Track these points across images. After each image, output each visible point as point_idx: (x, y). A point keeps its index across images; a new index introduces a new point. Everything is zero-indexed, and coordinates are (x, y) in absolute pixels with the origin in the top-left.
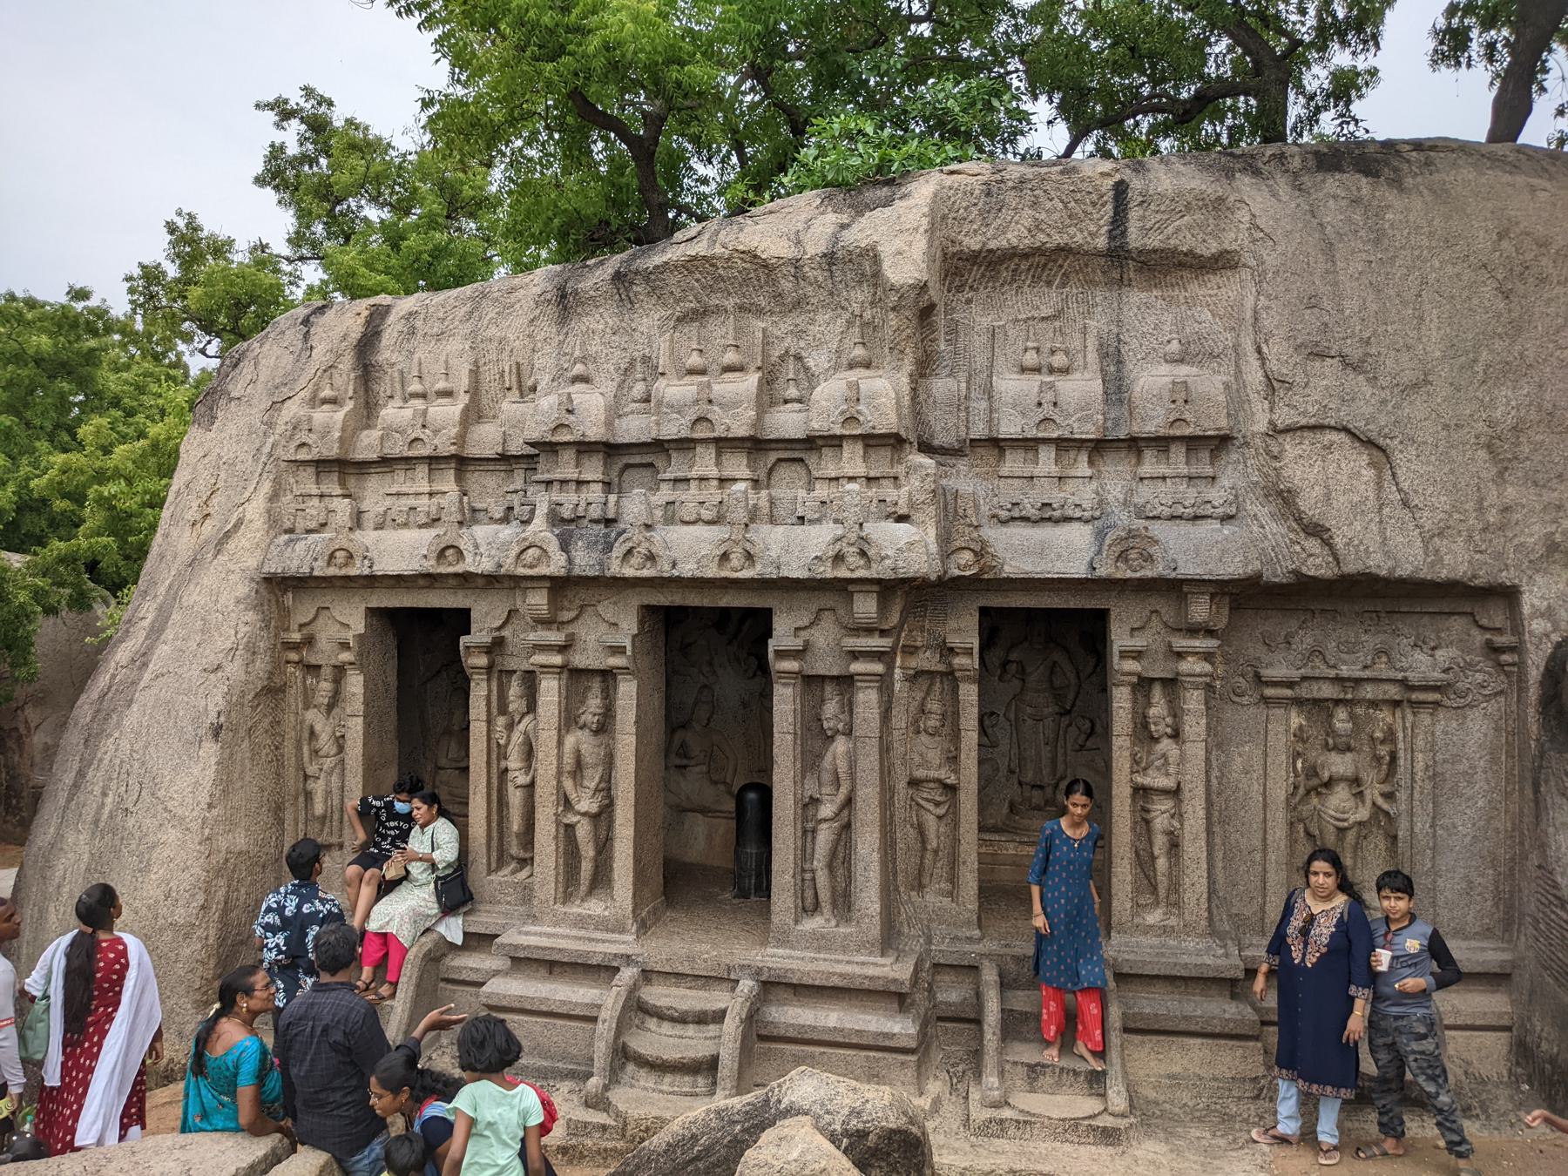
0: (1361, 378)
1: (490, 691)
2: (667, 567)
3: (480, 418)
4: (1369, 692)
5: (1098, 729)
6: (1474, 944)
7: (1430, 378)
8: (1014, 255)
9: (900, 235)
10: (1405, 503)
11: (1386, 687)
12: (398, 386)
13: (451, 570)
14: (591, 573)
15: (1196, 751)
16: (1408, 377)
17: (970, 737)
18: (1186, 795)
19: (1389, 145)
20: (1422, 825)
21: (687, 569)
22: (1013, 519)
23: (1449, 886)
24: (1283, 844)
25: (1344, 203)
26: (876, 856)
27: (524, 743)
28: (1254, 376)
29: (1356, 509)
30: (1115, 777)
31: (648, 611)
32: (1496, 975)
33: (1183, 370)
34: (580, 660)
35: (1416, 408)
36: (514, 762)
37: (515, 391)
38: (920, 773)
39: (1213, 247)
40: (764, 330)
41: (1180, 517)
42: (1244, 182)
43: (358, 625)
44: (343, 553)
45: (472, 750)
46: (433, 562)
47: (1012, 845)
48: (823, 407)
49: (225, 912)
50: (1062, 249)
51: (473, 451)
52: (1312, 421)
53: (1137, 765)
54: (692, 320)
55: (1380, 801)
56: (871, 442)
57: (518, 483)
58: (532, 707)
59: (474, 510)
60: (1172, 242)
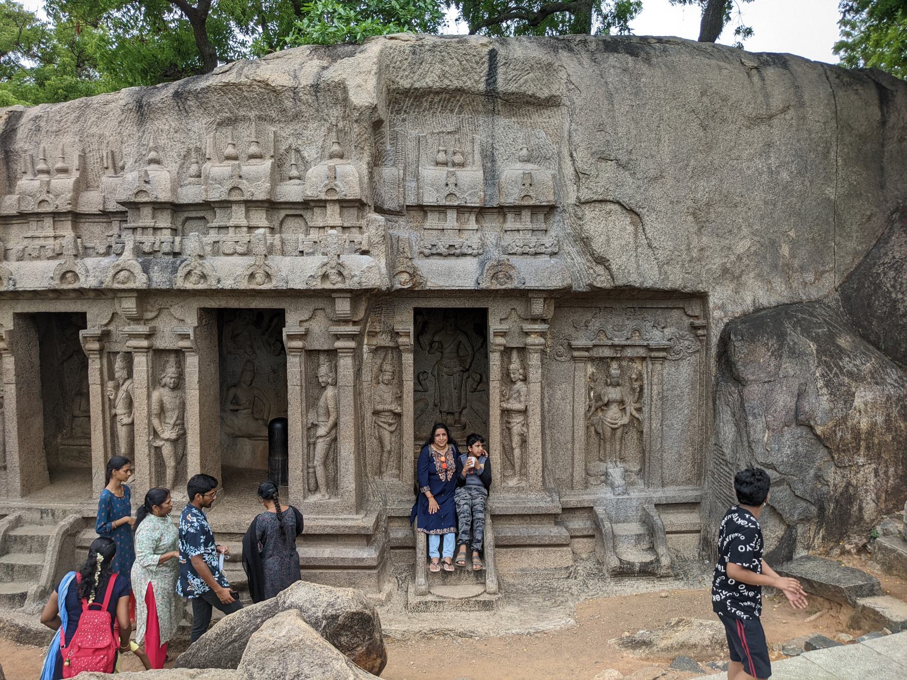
0: (627, 173)
1: (102, 365)
2: (214, 282)
3: (88, 187)
4: (629, 353)
5: (484, 379)
6: (682, 487)
7: (664, 174)
8: (431, 92)
9: (360, 75)
10: (650, 246)
11: (638, 349)
12: (29, 165)
13: (70, 287)
14: (164, 287)
15: (536, 388)
16: (652, 173)
17: (409, 384)
18: (530, 413)
19: (644, 39)
20: (655, 424)
21: (228, 284)
22: (433, 254)
23: (670, 457)
24: (583, 438)
25: (619, 71)
26: (352, 456)
27: (126, 397)
28: (569, 170)
29: (624, 248)
30: (491, 405)
31: (204, 313)
32: (693, 503)
33: (529, 167)
34: (160, 344)
35: (656, 192)
36: (120, 409)
37: (111, 170)
38: (380, 407)
39: (544, 93)
40: (275, 133)
41: (527, 254)
42: (564, 55)
45: (91, 403)
46: (57, 282)
48: (313, 181)
50: (459, 90)
51: (83, 209)
52: (600, 197)
53: (504, 397)
54: (227, 124)
55: (634, 413)
56: (344, 205)
57: (115, 230)
58: (130, 375)
59: (86, 248)
60: (523, 88)
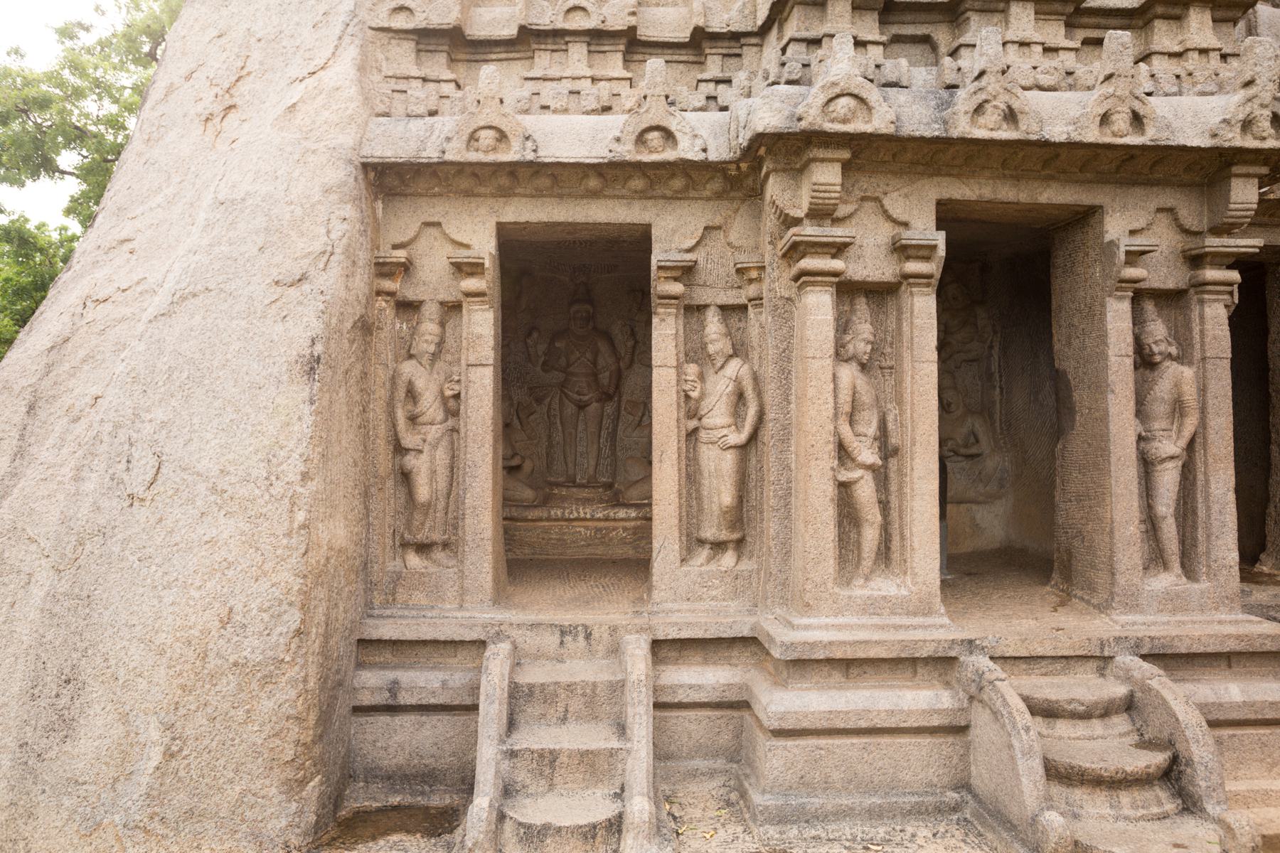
13: (655, 157)
43: (484, 246)
44: (491, 133)
49: (327, 637)
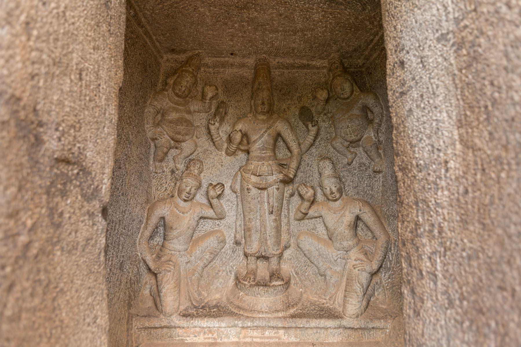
47: (233, 331)
